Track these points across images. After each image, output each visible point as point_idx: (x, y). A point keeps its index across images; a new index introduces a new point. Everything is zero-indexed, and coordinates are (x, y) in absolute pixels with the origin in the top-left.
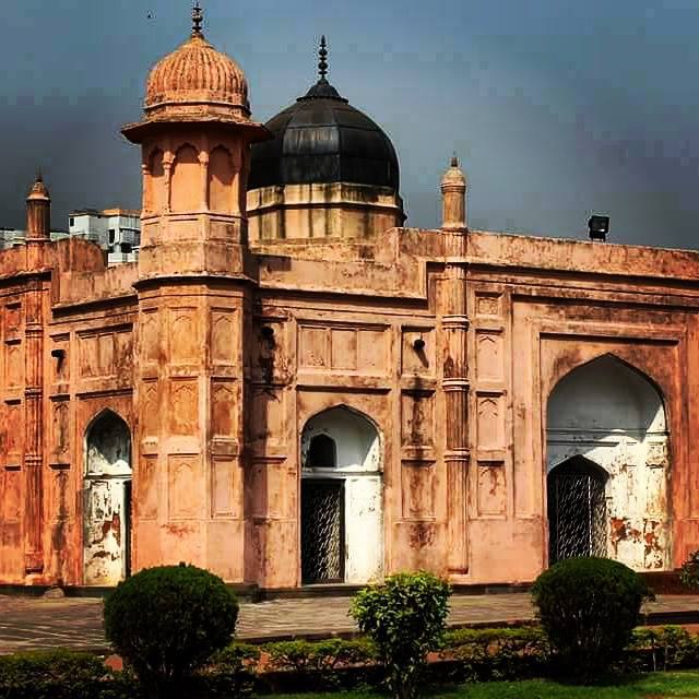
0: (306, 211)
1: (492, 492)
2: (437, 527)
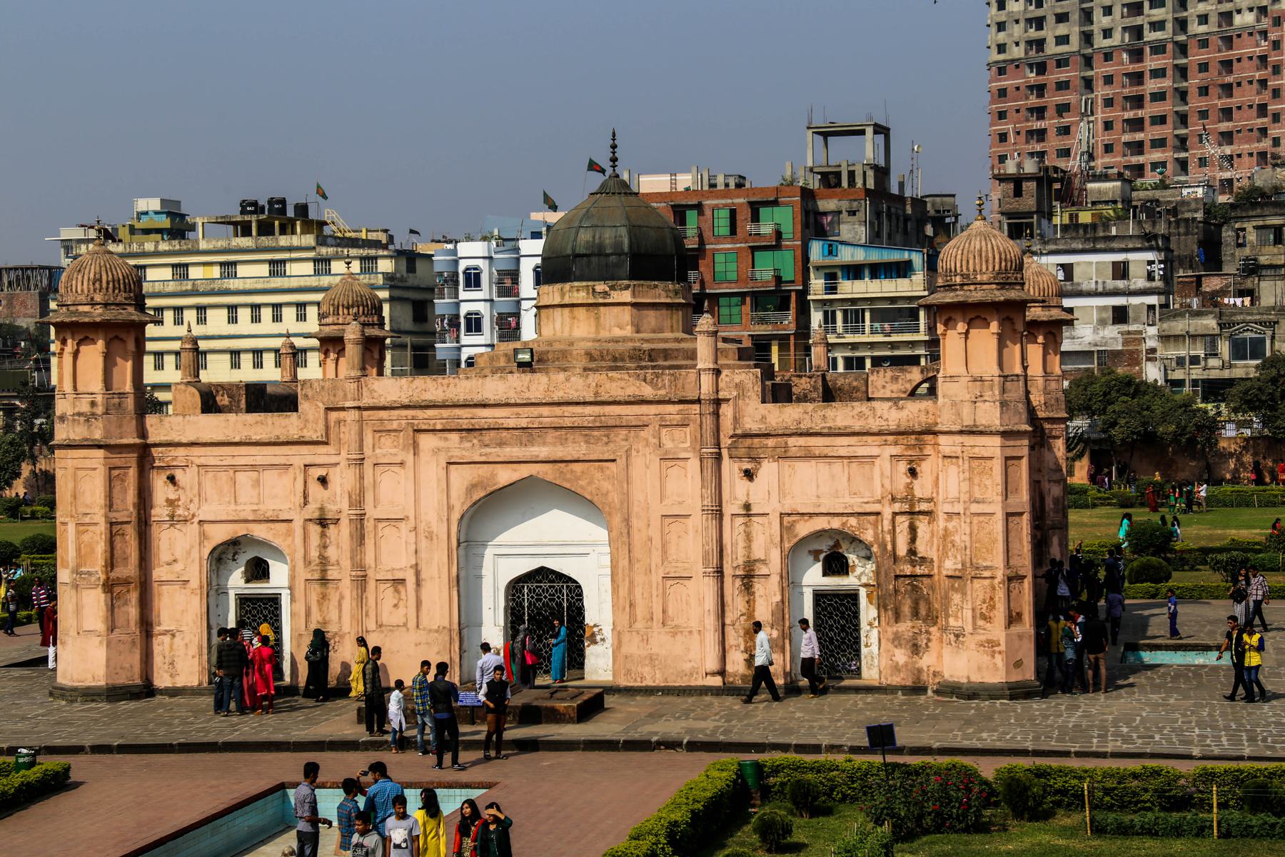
0: (566, 310)
1: (395, 606)
2: (342, 637)
